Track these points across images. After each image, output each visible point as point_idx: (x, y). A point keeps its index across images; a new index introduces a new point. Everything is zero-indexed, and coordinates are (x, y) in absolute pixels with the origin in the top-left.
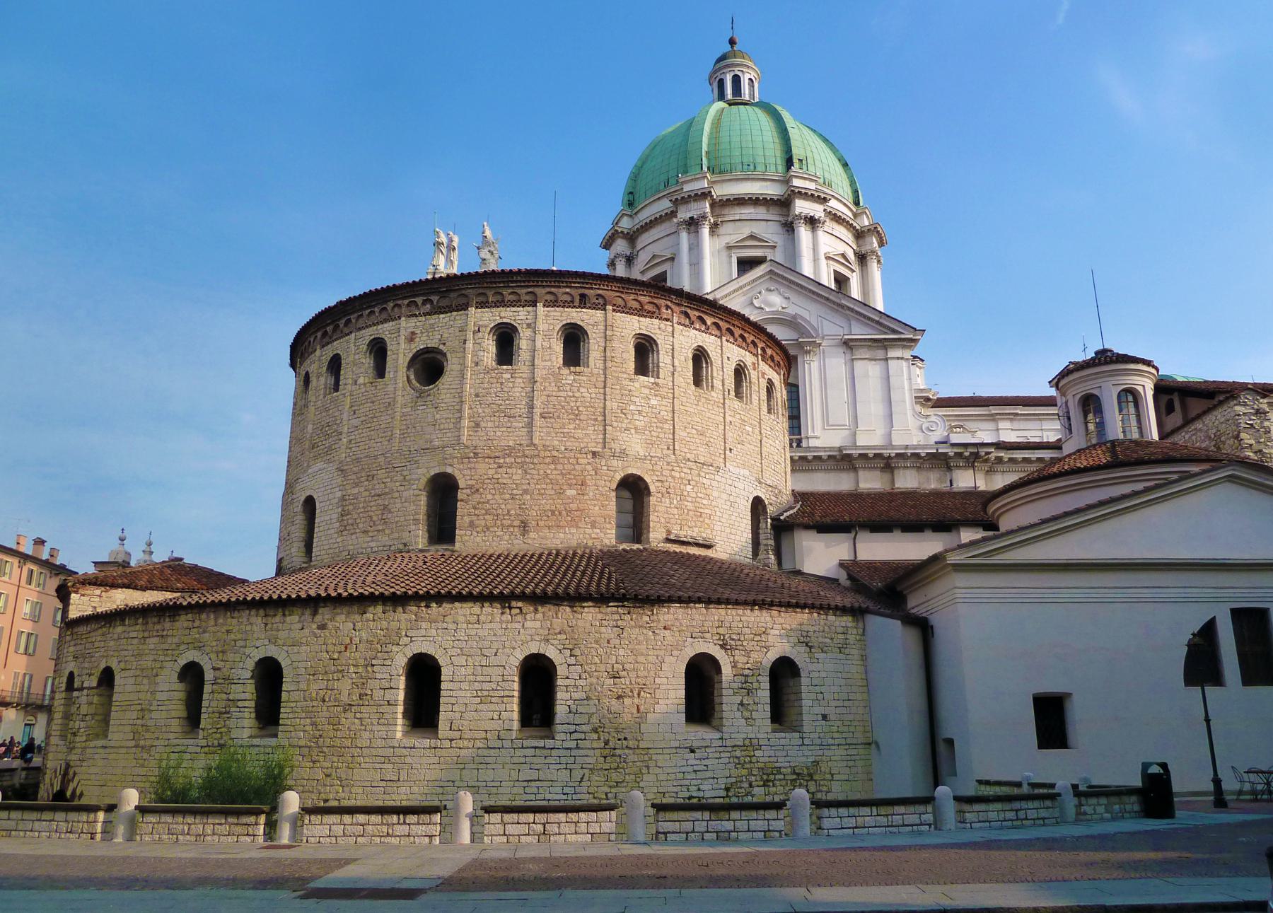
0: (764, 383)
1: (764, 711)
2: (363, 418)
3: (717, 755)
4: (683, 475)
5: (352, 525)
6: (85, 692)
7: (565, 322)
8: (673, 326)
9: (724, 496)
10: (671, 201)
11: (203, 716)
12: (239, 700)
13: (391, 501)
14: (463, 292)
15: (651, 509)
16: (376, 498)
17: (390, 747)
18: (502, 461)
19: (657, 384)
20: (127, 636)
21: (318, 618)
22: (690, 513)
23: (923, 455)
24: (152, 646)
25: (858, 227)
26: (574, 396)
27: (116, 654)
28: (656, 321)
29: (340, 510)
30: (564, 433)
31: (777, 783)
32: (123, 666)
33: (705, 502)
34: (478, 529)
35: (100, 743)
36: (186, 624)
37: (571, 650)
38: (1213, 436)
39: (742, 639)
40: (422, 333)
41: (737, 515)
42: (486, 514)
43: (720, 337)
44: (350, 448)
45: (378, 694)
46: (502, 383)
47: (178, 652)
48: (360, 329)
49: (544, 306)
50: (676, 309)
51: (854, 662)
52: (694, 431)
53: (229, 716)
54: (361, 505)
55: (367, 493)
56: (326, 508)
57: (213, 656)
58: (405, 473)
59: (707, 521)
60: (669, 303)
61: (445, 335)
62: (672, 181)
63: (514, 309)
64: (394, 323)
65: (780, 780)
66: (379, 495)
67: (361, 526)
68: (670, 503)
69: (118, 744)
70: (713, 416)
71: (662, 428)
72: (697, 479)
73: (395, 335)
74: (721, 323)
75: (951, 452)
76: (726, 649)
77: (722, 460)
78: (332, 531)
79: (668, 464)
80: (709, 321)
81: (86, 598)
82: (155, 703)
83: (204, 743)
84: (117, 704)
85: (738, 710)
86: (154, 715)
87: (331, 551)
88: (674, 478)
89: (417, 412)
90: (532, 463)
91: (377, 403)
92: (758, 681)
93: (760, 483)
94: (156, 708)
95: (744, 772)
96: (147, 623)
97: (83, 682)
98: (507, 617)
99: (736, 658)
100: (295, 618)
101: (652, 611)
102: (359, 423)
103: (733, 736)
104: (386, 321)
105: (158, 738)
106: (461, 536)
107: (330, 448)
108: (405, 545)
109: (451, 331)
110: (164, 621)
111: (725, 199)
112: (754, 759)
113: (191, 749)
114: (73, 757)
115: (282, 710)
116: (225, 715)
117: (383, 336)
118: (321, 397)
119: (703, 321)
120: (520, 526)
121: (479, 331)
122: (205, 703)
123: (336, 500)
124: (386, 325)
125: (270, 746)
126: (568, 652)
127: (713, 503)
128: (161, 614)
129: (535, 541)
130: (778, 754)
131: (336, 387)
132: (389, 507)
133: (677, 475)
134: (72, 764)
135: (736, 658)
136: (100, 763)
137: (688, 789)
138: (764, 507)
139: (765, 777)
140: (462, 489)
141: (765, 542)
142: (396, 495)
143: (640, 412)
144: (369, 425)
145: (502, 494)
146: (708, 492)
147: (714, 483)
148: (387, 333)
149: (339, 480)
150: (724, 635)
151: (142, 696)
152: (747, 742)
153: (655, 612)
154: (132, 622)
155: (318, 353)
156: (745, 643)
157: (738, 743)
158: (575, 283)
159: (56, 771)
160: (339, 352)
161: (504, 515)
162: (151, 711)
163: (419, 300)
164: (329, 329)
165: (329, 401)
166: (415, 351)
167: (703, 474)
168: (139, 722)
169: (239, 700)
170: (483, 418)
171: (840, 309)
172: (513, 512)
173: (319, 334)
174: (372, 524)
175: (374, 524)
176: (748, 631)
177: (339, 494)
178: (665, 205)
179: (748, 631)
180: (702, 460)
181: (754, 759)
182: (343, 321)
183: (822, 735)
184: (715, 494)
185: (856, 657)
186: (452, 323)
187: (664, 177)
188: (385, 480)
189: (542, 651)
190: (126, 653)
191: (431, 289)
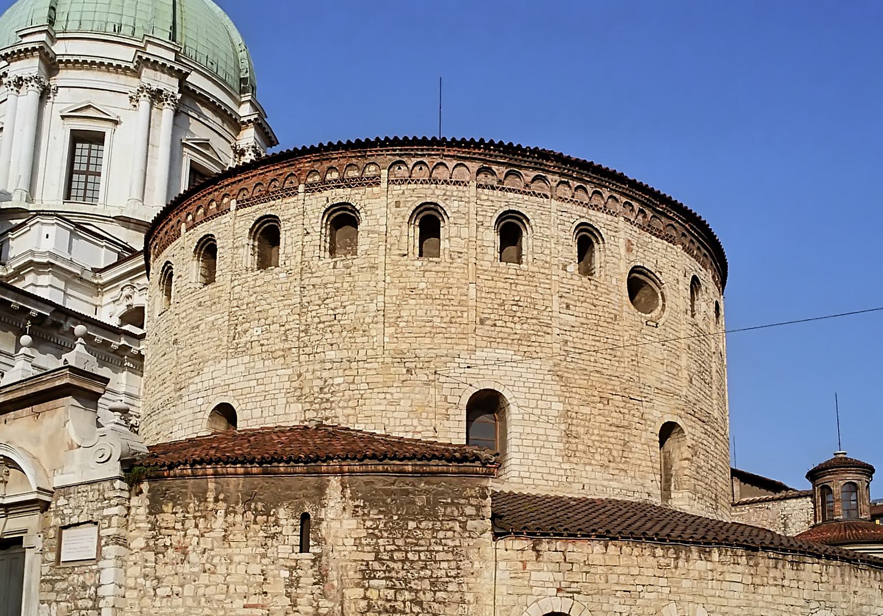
2: (584, 321)
27: (702, 600)
29: (563, 427)
55: (603, 420)
67: (597, 457)
91: (600, 308)
96: (757, 565)
102: (577, 324)
166: (633, 264)
177: (560, 407)
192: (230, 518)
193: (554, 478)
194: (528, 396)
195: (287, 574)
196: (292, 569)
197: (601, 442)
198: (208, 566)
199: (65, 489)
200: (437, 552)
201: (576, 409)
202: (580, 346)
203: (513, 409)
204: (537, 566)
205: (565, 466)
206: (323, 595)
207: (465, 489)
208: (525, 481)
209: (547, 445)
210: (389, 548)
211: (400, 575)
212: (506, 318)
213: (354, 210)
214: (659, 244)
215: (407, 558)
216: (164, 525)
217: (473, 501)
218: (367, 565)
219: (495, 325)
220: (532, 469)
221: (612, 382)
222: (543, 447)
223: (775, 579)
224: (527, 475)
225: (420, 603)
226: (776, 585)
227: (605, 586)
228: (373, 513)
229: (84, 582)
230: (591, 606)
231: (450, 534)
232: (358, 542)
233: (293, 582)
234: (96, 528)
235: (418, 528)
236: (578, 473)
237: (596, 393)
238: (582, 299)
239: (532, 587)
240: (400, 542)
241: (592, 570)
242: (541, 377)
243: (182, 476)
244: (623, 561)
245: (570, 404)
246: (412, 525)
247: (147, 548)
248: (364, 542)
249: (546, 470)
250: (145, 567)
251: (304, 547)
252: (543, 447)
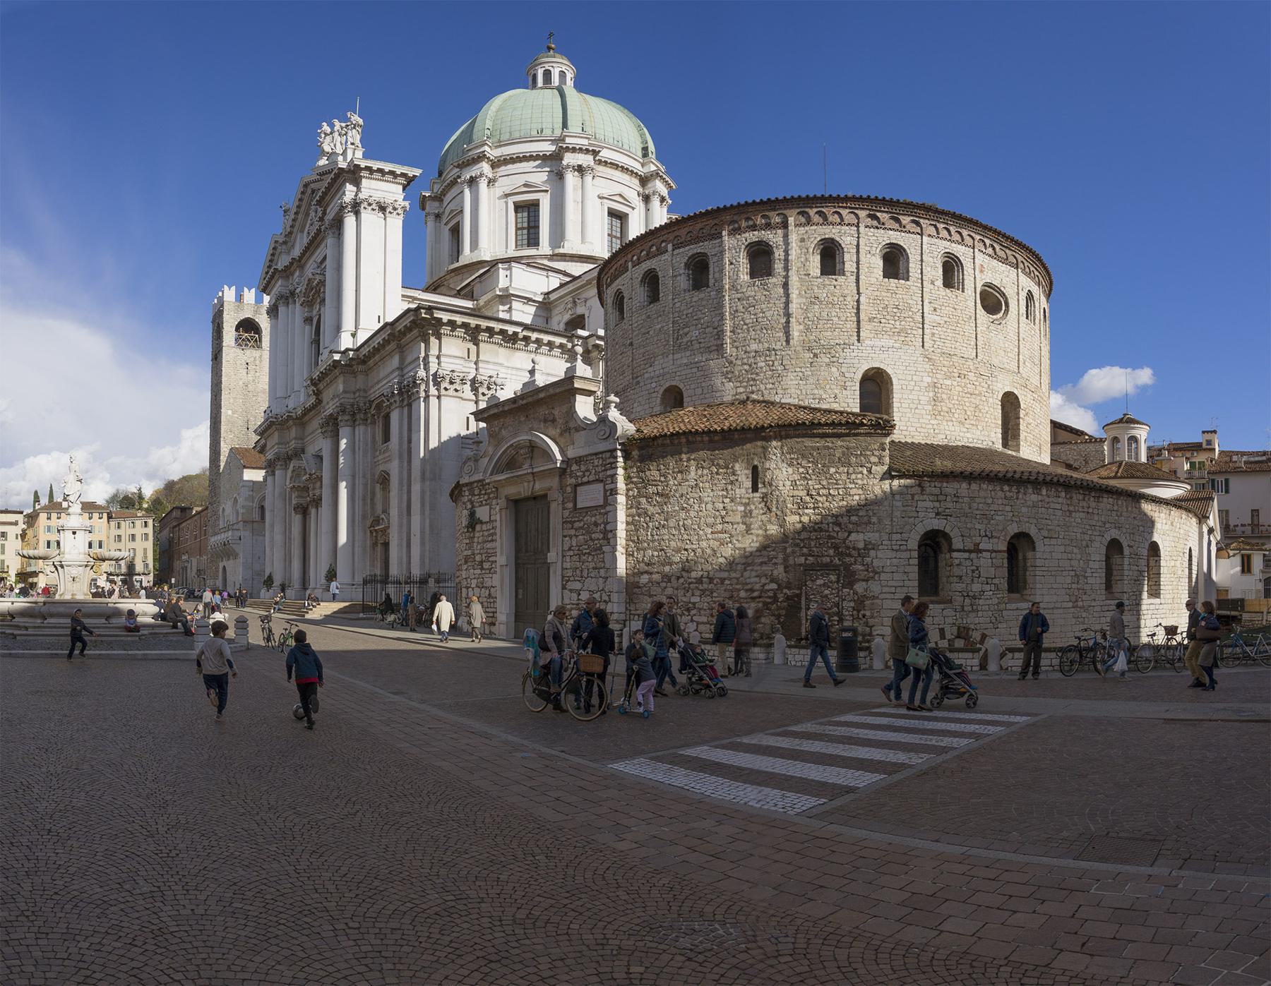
14: (856, 211)
29: (931, 394)
32: (1045, 533)
54: (955, 398)
55: (961, 390)
67: (956, 416)
82: (1089, 570)
86: (1090, 580)
87: (923, 430)
94: (1091, 575)
132: (981, 407)
151: (1074, 563)
162: (1086, 578)
168: (1074, 586)
177: (929, 380)
192: (700, 472)
193: (925, 430)
194: (905, 372)
195: (743, 508)
196: (746, 505)
198: (685, 505)
199: (578, 460)
200: (851, 489)
201: (941, 382)
203: (895, 381)
204: (921, 498)
205: (933, 422)
206: (770, 521)
207: (870, 444)
208: (904, 433)
209: (919, 407)
210: (816, 487)
211: (825, 506)
213: (767, 245)
215: (830, 494)
216: (652, 478)
217: (876, 453)
218: (801, 499)
220: (909, 424)
222: (916, 408)
224: (905, 428)
225: (839, 525)
227: (970, 511)
228: (804, 463)
229: (595, 522)
230: (959, 524)
231: (860, 476)
232: (794, 484)
233: (748, 514)
234: (602, 484)
235: (837, 472)
236: (942, 427)
237: (955, 370)
239: (918, 512)
240: (824, 483)
241: (960, 500)
242: (915, 359)
243: (663, 445)
244: (982, 494)
246: (832, 470)
247: (640, 495)
248: (798, 483)
249: (919, 425)
250: (639, 509)
251: (755, 489)
252: (916, 408)
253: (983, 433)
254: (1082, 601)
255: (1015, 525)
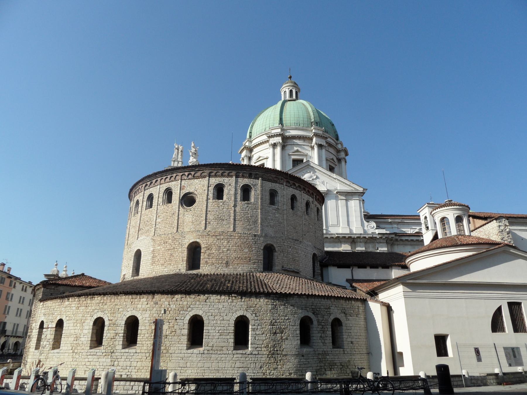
0: (316, 209)
1: (329, 340)
2: (163, 219)
3: (312, 358)
4: (288, 244)
5: (157, 261)
6: (49, 329)
7: (244, 184)
8: (284, 186)
9: (303, 253)
10: (267, 136)
11: (104, 340)
12: (120, 333)
13: (174, 252)
15: (276, 258)
16: (167, 251)
17: (183, 353)
18: (219, 237)
19: (278, 209)
20: (70, 306)
21: (154, 300)
22: (291, 259)
23: (367, 237)
24: (82, 311)
25: (338, 149)
26: (247, 213)
27: (65, 313)
28: (278, 184)
30: (243, 227)
31: (335, 369)
32: (68, 318)
33: (296, 255)
34: (209, 264)
35: (56, 351)
36: (98, 301)
37: (256, 314)
38: (487, 234)
39: (321, 310)
40: (187, 186)
41: (307, 260)
42: (213, 258)
43: (301, 191)
44: (157, 231)
45: (178, 331)
46: (219, 207)
47: (93, 313)
48: (162, 184)
49: (236, 178)
50: (285, 180)
51: (362, 320)
52: (292, 227)
53: (115, 340)
54: (161, 254)
55: (163, 249)
56: (146, 254)
57: (109, 315)
58: (180, 241)
59: (297, 262)
60: (282, 178)
61: (197, 187)
62: (267, 129)
63: (224, 178)
64: (176, 182)
65: (336, 368)
66: (169, 250)
67: (161, 262)
68: (283, 255)
69: (65, 351)
70: (298, 222)
71: (280, 226)
72: (293, 246)
73: (177, 187)
74: (301, 186)
75: (378, 237)
76: (315, 315)
77: (302, 239)
78: (149, 264)
79: (283, 240)
80: (297, 185)
81: (48, 290)
82: (82, 334)
83: (104, 351)
84: (65, 334)
85: (320, 339)
86: (83, 339)
87: (148, 272)
88: (285, 245)
89: (185, 217)
90: (231, 238)
91: (168, 213)
92: (327, 328)
93: (315, 248)
95: (322, 365)
96: (80, 301)
97: (48, 325)
98: (230, 300)
99: (319, 318)
100: (145, 300)
101: (287, 299)
103: (318, 350)
104: (172, 181)
105: (83, 349)
106: (202, 267)
107: (148, 230)
108: (179, 270)
109: (199, 186)
110: (88, 299)
111: (288, 136)
112: (326, 359)
113: (98, 354)
114: (42, 358)
115: (138, 338)
116: (113, 340)
117: (171, 187)
118: (145, 210)
119: (295, 185)
120: (225, 263)
121: (210, 186)
122: (105, 334)
123: (151, 251)
124: (173, 183)
125: (133, 353)
126: (254, 315)
127: (299, 256)
128: (86, 297)
129: (232, 269)
130: (335, 357)
131: (151, 206)
133: (286, 244)
134: (41, 360)
135: (319, 318)
136: (56, 359)
137: (302, 372)
138: (317, 257)
139: (331, 367)
140: (204, 248)
141: (317, 271)
142: (176, 250)
143: (272, 219)
144: (165, 222)
145: (219, 250)
146: (298, 251)
147: (299, 248)
148: (173, 186)
149: (152, 243)
150: (314, 309)
152: (324, 352)
153: (288, 299)
154: (73, 300)
155: (143, 192)
156: (322, 312)
157: (320, 353)
158: (247, 169)
159: (33, 363)
160: (152, 192)
161: (220, 259)
163: (186, 174)
164: (149, 183)
165: (148, 212)
166: (184, 193)
167: (295, 244)
168: (75, 342)
169: (120, 333)
170: (211, 220)
171: (335, 180)
172: (223, 258)
173: (144, 185)
174: (165, 261)
175: (167, 261)
176: (323, 307)
177: (152, 249)
178: (265, 138)
179: (323, 307)
180: (295, 238)
181: (326, 359)
182: (155, 180)
183: (351, 350)
184: (300, 252)
185: (362, 319)
186: (199, 183)
187: (264, 127)
188: (171, 244)
189: (245, 314)
190: (69, 313)
191: (191, 169)
197: (162, 256)
202: (161, 228)
205: (151, 267)
209: (148, 262)
212: (145, 227)
214: (196, 181)
219: (142, 230)
221: (169, 236)
223: (84, 304)
226: (85, 306)
238: (163, 212)
245: (155, 247)
253: (174, 267)
254: (77, 350)
255: (59, 316)
